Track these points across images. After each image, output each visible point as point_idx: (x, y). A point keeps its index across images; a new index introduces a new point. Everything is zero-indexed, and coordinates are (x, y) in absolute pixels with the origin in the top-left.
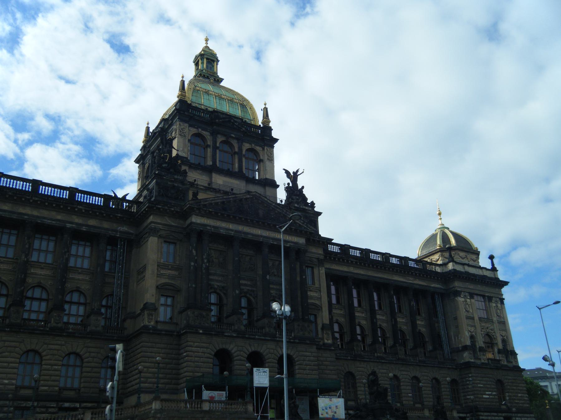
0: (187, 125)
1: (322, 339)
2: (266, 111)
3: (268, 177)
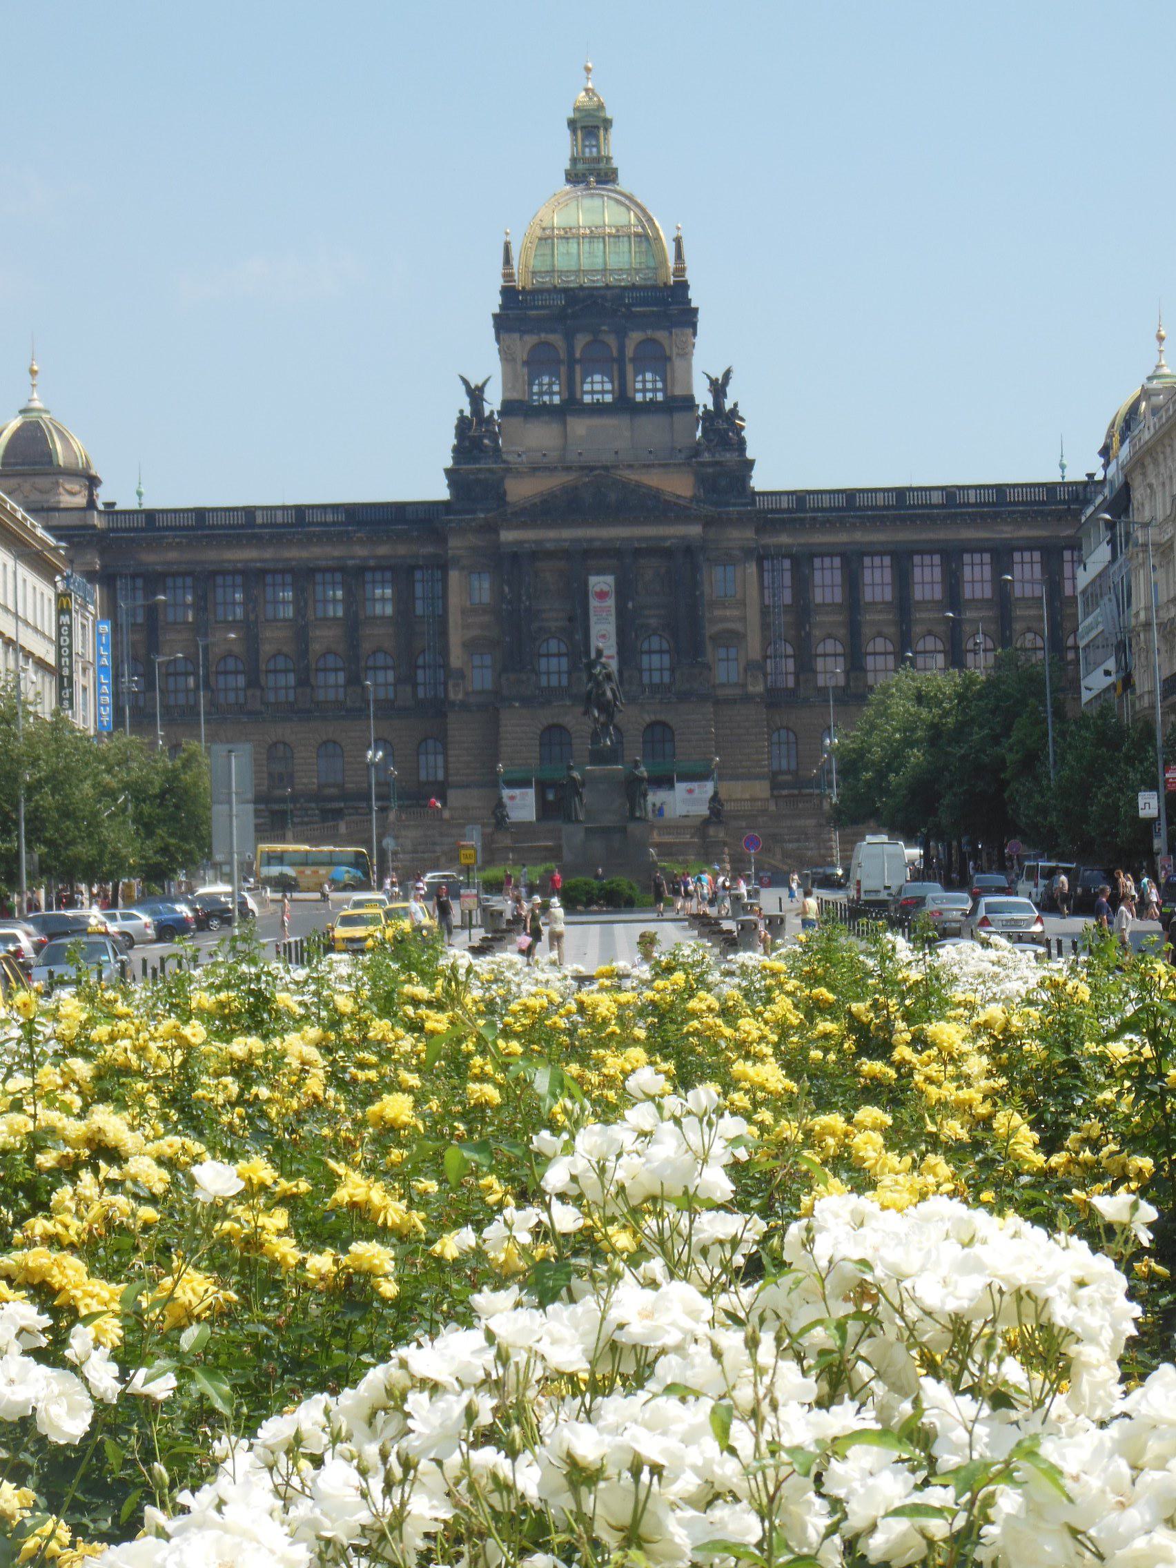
0: (516, 336)
1: (744, 686)
2: (678, 241)
3: (678, 391)
